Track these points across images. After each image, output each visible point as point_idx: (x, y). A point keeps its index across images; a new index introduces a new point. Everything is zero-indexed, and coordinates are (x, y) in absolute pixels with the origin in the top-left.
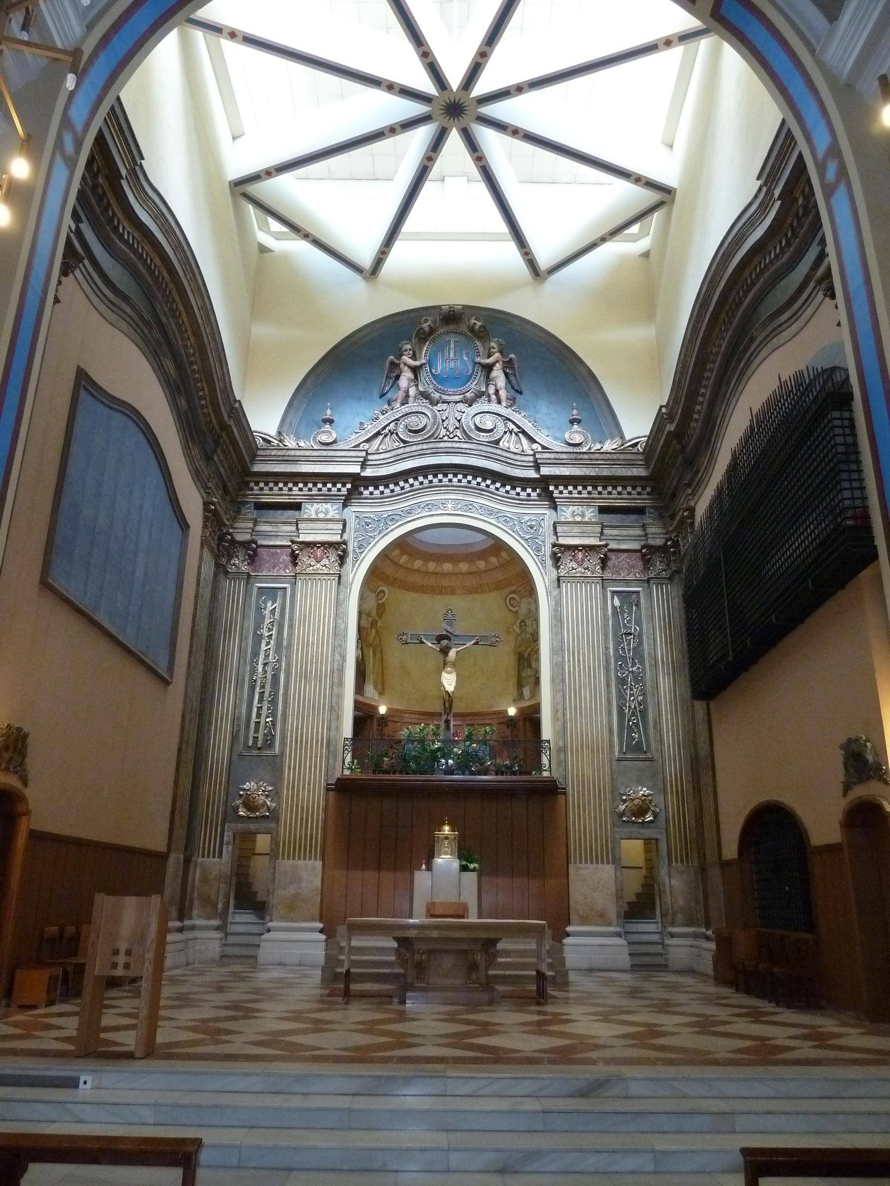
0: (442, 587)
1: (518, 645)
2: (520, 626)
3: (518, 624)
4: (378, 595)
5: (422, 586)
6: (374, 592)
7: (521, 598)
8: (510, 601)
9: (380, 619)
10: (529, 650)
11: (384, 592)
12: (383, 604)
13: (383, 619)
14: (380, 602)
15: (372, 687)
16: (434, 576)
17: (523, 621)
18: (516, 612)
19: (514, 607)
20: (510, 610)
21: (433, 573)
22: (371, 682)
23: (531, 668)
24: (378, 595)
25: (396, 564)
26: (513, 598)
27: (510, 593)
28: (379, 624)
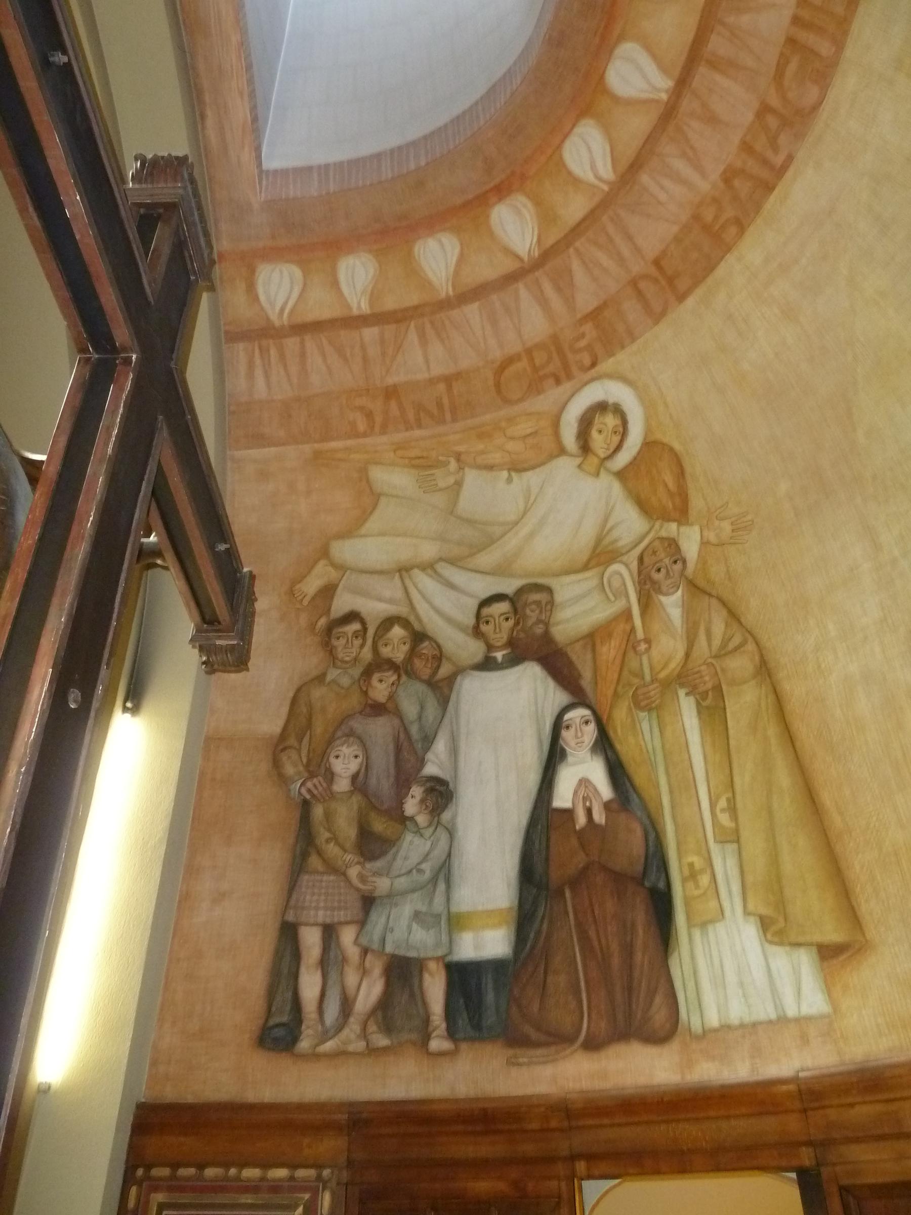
0: (791, 41)
4: (585, 447)
5: (728, 177)
6: (562, 451)
9: (682, 514)
11: (618, 410)
12: (649, 445)
13: (697, 503)
14: (623, 459)
15: (750, 932)
16: (703, 75)
21: (682, 83)
22: (732, 902)
24: (585, 447)
25: (511, 278)
28: (690, 545)
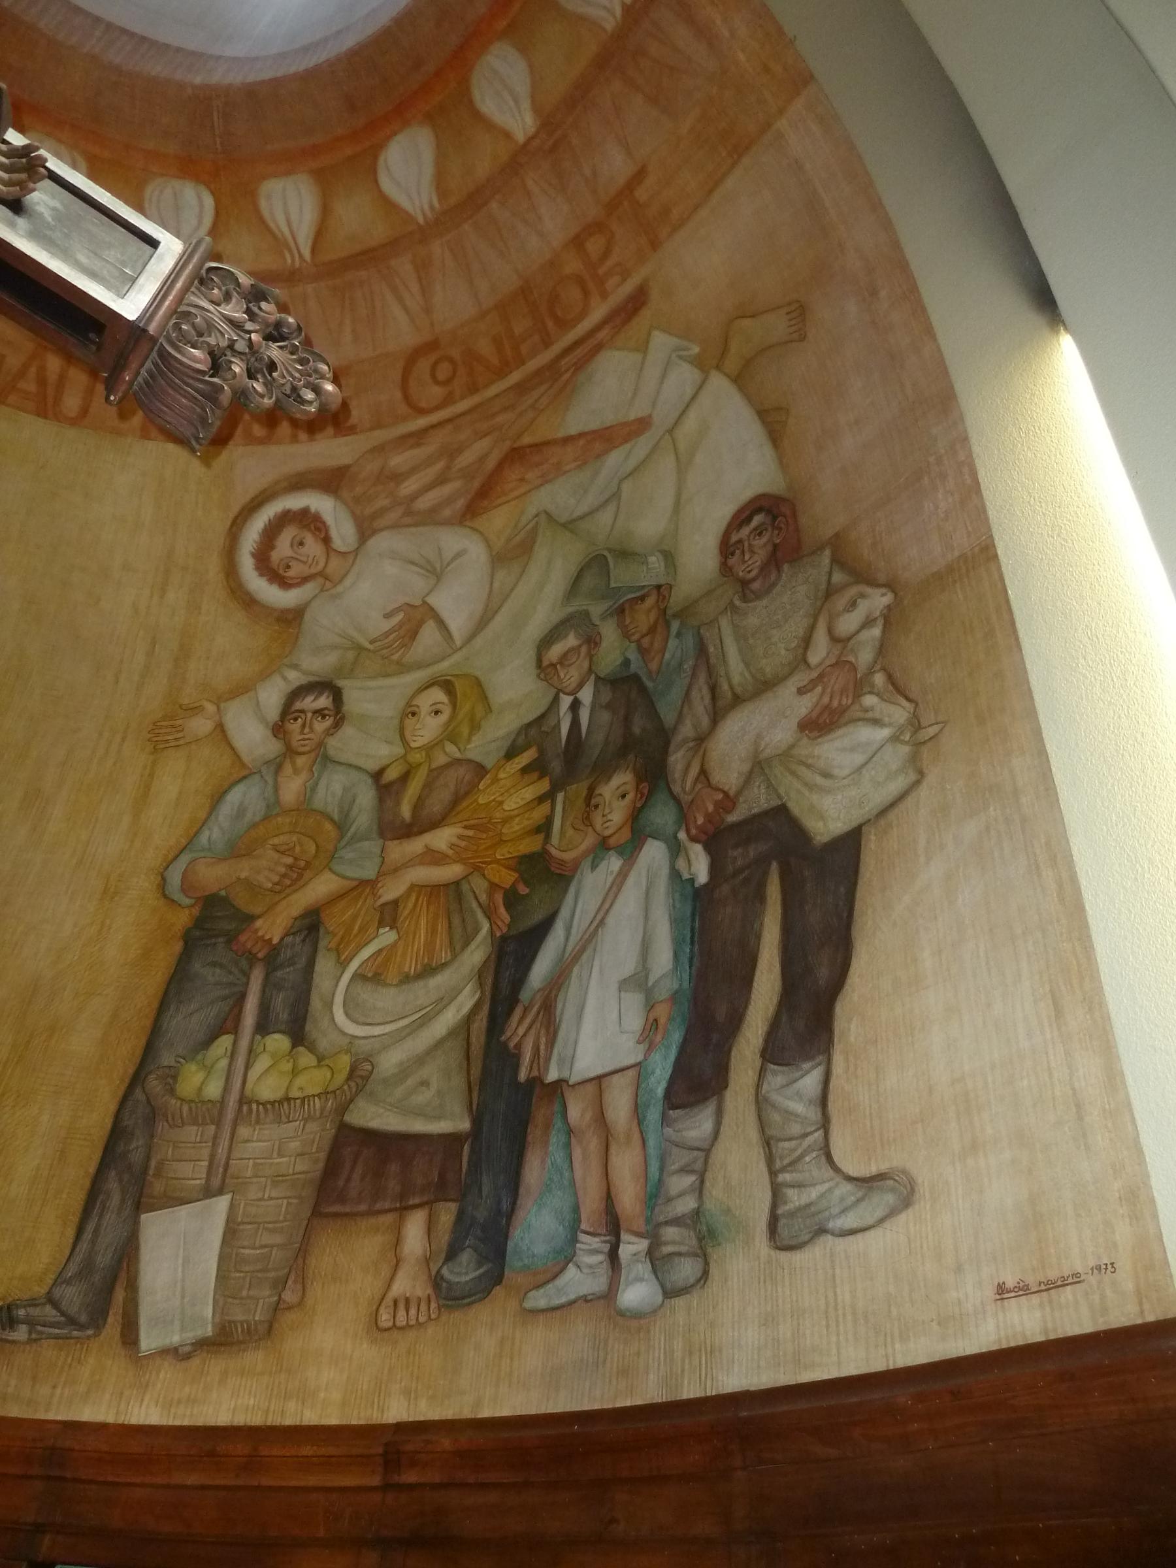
1: (215, 834)
2: (288, 710)
3: (272, 696)
7: (365, 531)
8: (271, 534)
10: (321, 887)
17: (327, 686)
18: (292, 619)
19: (284, 583)
20: (249, 602)
23: (298, 1035)
26: (308, 520)
27: (298, 483)
